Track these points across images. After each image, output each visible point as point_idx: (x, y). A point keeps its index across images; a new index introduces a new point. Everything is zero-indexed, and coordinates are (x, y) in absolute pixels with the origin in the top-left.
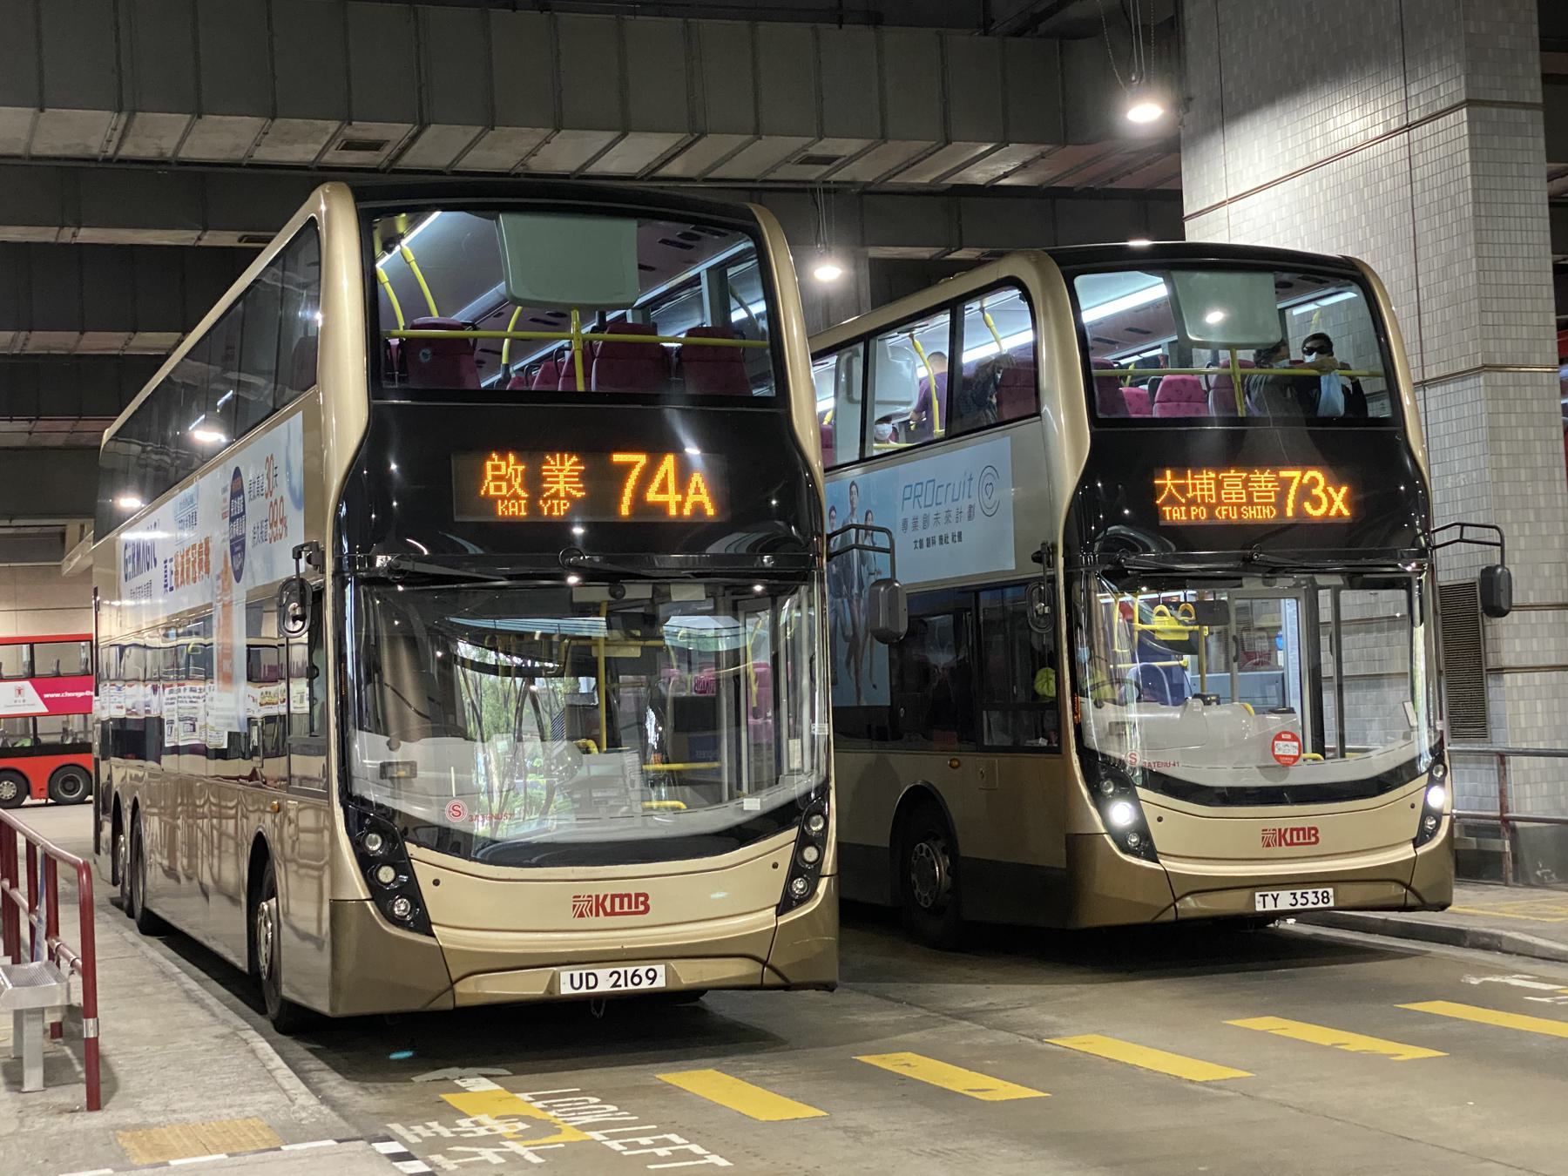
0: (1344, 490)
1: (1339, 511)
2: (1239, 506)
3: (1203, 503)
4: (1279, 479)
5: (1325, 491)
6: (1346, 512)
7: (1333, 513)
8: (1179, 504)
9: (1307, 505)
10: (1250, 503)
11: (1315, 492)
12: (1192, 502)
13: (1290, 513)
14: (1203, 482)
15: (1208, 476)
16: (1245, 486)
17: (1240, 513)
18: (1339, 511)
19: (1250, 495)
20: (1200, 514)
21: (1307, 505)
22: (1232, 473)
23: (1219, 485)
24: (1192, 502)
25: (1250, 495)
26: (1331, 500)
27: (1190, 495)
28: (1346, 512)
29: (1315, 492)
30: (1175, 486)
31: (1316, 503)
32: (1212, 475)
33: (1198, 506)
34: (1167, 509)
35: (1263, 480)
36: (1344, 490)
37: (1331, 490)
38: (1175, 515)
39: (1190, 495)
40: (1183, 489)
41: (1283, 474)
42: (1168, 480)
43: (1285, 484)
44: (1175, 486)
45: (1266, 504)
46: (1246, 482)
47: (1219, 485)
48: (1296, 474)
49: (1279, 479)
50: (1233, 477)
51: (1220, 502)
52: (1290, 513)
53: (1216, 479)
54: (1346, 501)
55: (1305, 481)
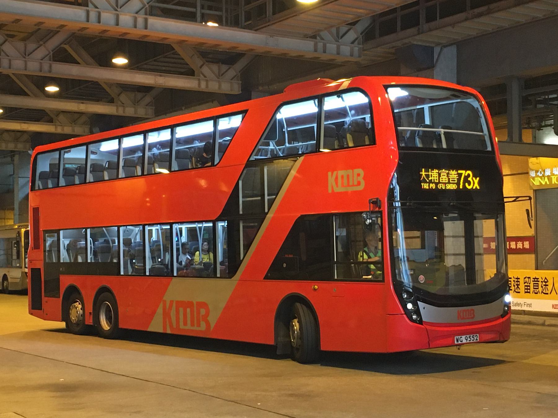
0: (478, 179)
1: (476, 187)
2: (445, 183)
3: (434, 182)
4: (458, 174)
5: (472, 179)
6: (478, 188)
7: (474, 188)
8: (426, 182)
9: (467, 184)
10: (449, 183)
11: (470, 179)
12: (431, 182)
13: (461, 187)
14: (434, 174)
15: (436, 171)
16: (448, 176)
17: (446, 187)
18: (476, 187)
19: (449, 179)
20: (433, 186)
21: (467, 184)
22: (444, 170)
23: (439, 175)
24: (431, 182)
25: (449, 179)
26: (475, 184)
27: (430, 179)
28: (478, 188)
29: (470, 179)
30: (426, 175)
31: (469, 185)
32: (437, 171)
33: (433, 183)
34: (422, 184)
35: (453, 174)
36: (478, 179)
37: (474, 178)
38: (425, 186)
39: (430, 179)
40: (428, 176)
41: (459, 172)
42: (423, 173)
43: (460, 175)
44: (426, 175)
45: (454, 183)
46: (448, 174)
47: (439, 175)
48: (463, 172)
49: (458, 174)
50: (444, 172)
51: (439, 183)
52: (461, 187)
53: (438, 173)
54: (479, 183)
55: (466, 175)
